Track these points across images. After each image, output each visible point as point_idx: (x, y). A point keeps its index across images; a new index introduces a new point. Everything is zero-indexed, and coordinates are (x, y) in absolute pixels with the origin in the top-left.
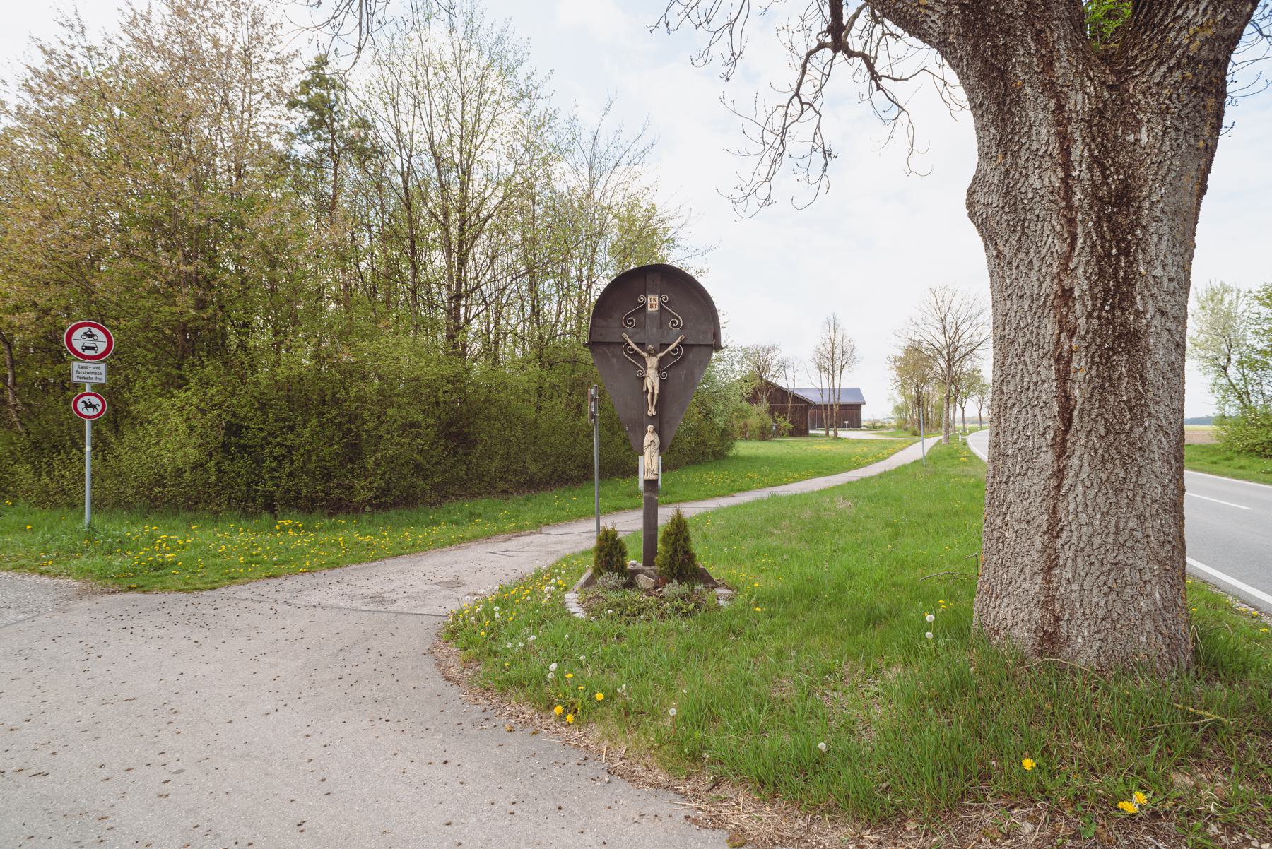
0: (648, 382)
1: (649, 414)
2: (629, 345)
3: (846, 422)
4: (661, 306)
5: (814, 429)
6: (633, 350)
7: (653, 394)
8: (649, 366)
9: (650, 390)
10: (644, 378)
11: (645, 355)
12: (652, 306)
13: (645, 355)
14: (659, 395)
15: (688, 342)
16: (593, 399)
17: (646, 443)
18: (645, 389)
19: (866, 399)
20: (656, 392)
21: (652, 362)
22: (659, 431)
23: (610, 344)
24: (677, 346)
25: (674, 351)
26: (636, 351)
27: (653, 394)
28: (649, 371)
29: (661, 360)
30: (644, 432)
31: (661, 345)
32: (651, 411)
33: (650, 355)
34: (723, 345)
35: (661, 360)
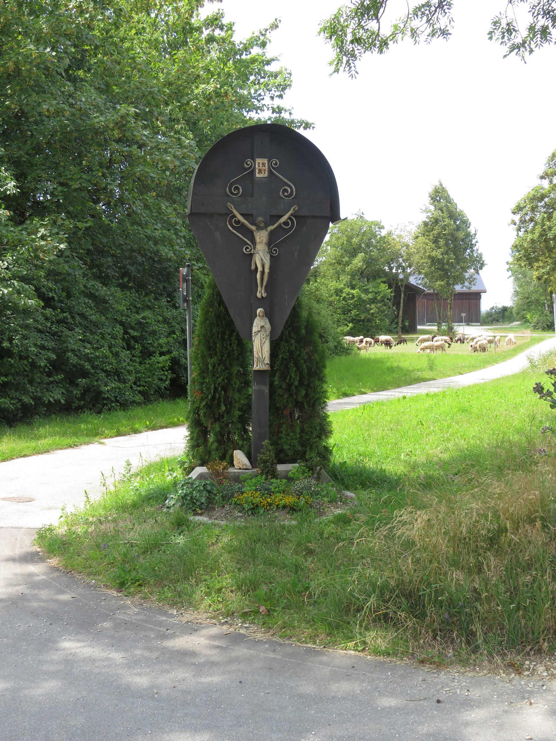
0: (257, 259)
1: (259, 295)
2: (234, 216)
3: (463, 315)
4: (270, 172)
5: (423, 324)
6: (238, 222)
7: (263, 273)
8: (258, 240)
9: (260, 269)
10: (251, 255)
11: (253, 228)
12: (260, 171)
13: (253, 228)
14: (270, 274)
15: (302, 213)
16: (186, 280)
17: (255, 329)
18: (253, 267)
19: (487, 288)
20: (267, 270)
21: (261, 237)
22: (269, 315)
23: (211, 215)
24: (289, 218)
25: (286, 223)
26: (243, 224)
27: (263, 273)
28: (259, 247)
29: (271, 233)
30: (253, 316)
31: (270, 216)
32: (261, 293)
33: (259, 228)
34: (342, 216)
35: (272, 234)
